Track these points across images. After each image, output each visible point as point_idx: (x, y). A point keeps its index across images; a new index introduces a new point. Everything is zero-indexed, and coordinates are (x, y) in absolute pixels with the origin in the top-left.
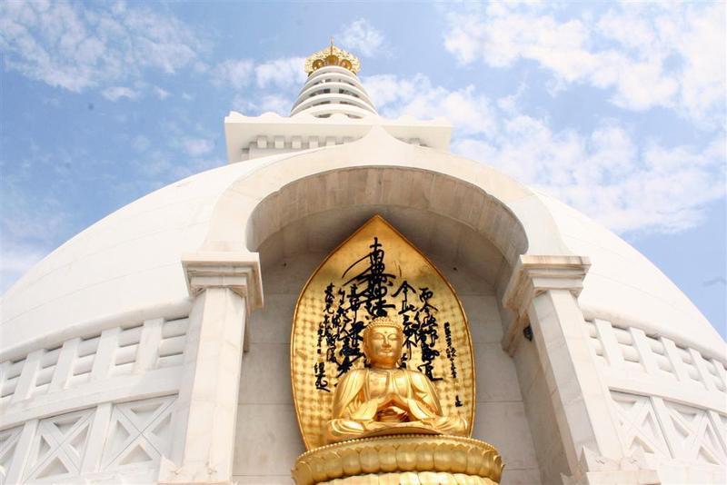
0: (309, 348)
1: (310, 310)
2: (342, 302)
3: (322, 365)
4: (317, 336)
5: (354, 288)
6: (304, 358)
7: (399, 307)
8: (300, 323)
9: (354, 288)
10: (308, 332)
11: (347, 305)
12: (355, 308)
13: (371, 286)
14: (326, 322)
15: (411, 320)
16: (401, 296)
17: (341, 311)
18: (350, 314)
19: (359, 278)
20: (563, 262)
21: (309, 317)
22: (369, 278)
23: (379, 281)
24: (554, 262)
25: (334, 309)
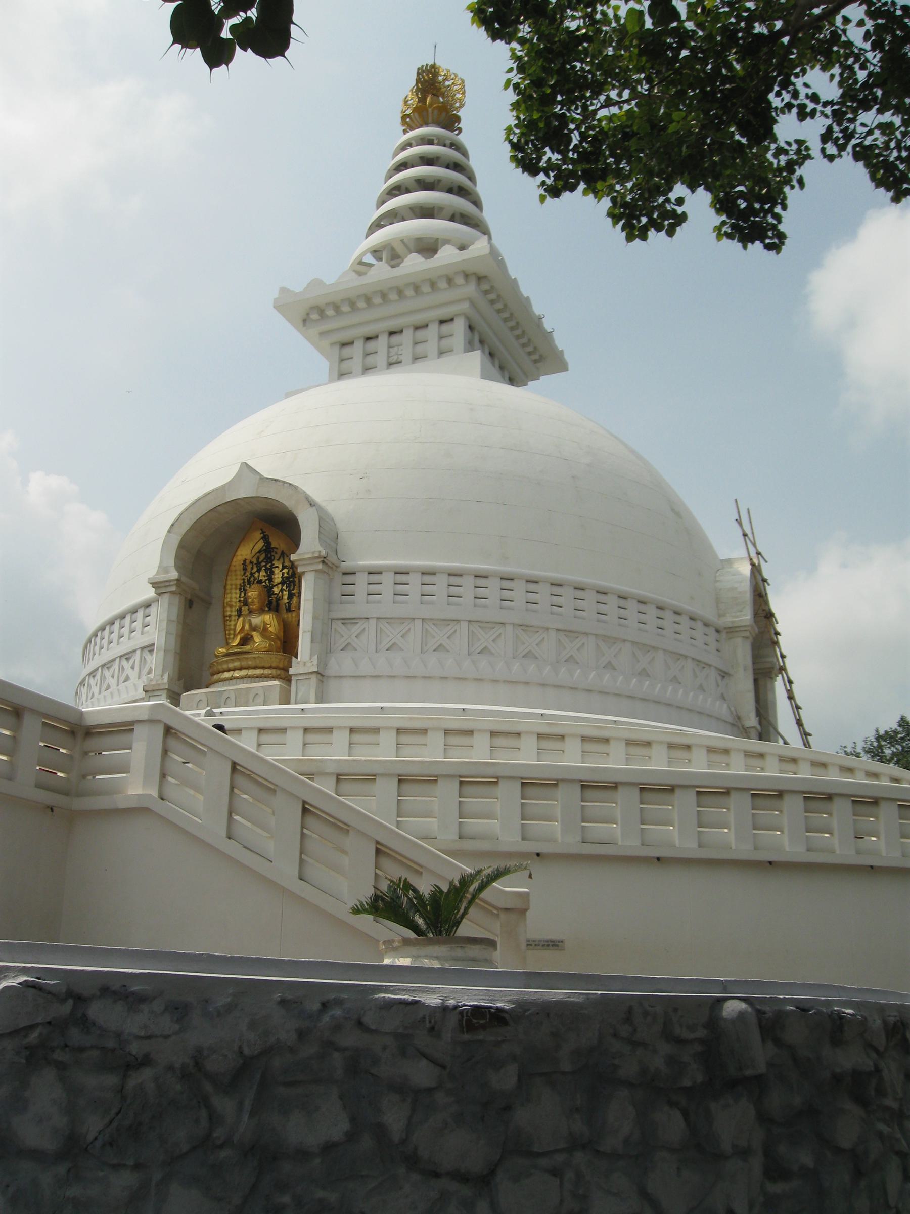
0: (234, 600)
1: (234, 577)
2: (252, 568)
3: (240, 609)
4: (238, 591)
5: (258, 558)
6: (231, 606)
7: (281, 567)
8: (228, 587)
9: (258, 558)
10: (233, 591)
11: (255, 569)
12: (259, 571)
13: (266, 556)
14: (244, 582)
15: (286, 575)
16: (281, 560)
17: (252, 574)
18: (256, 575)
19: (259, 552)
20: (310, 556)
21: (234, 582)
22: (265, 551)
23: (270, 552)
24: (307, 556)
25: (248, 574)
